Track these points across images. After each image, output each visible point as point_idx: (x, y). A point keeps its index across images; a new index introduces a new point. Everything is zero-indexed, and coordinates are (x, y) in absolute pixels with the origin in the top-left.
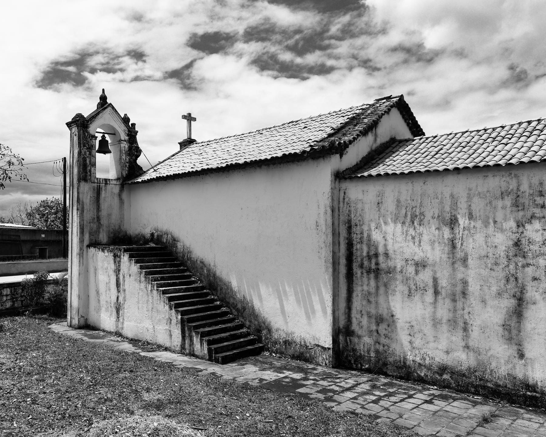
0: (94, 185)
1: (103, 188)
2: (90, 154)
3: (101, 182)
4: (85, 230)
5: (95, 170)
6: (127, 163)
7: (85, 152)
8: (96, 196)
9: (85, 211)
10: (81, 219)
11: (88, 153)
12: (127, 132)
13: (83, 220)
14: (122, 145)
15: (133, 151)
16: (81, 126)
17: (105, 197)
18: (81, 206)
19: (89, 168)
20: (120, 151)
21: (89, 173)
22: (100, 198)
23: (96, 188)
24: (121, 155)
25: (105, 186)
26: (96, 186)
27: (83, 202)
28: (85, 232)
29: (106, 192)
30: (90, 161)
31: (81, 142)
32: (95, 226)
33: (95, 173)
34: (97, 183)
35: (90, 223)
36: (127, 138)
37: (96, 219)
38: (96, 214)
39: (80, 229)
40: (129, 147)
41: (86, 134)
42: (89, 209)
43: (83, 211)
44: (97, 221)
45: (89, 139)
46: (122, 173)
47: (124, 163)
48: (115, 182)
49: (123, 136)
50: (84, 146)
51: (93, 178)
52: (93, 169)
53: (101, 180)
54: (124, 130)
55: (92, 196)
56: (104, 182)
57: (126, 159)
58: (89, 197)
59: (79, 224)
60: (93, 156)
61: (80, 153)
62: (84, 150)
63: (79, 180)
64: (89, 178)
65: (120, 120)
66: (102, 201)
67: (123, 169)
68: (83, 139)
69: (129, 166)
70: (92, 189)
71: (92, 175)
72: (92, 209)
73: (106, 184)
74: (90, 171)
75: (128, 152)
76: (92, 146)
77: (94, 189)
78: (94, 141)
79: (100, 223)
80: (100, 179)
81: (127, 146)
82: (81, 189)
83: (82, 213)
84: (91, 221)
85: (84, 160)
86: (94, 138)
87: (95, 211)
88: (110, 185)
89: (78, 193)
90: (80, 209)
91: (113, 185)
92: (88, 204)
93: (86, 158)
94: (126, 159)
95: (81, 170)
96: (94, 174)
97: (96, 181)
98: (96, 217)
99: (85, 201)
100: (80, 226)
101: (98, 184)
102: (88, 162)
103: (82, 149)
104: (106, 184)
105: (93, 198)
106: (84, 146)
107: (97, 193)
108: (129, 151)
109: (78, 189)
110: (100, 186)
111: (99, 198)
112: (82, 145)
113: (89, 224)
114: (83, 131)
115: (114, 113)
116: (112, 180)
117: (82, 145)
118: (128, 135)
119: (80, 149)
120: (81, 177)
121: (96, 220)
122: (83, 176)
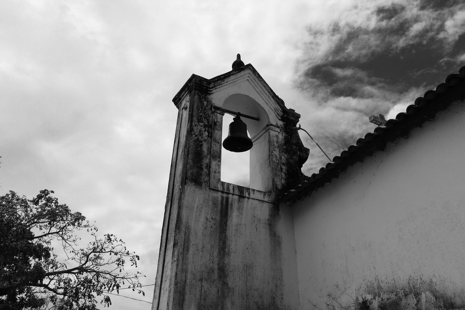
0: (215, 194)
1: (236, 205)
2: (210, 136)
3: (231, 191)
4: (187, 297)
5: (219, 166)
6: (283, 164)
7: (200, 131)
8: (218, 218)
9: (191, 252)
10: (180, 267)
11: (207, 133)
12: (281, 114)
13: (185, 271)
14: (272, 133)
15: (294, 147)
16: (196, 89)
17: (238, 225)
18: (182, 235)
19: (206, 161)
20: (269, 142)
21: (205, 170)
22: (229, 223)
23: (219, 202)
24: (272, 149)
25: (239, 201)
26: (220, 199)
27: (188, 228)
28: (186, 302)
29: (241, 214)
30: (209, 149)
31: (195, 113)
32: (214, 291)
33: (219, 172)
34: (223, 192)
35: (201, 280)
36: (280, 123)
37: (216, 272)
38: (216, 260)
39: (175, 292)
40: (285, 138)
41: (205, 103)
42: (200, 247)
43: (186, 248)
44: (220, 277)
45: (210, 112)
46: (273, 181)
47: (278, 164)
48: (260, 197)
49: (274, 119)
50: (199, 121)
51: (213, 182)
52: (214, 163)
53: (231, 188)
54: (276, 110)
55: (209, 217)
56: (237, 192)
57: (281, 158)
58: (202, 219)
59: (173, 279)
60: (215, 141)
61: (190, 131)
62: (199, 127)
63: (184, 183)
64: (206, 179)
65: (266, 92)
66: (231, 231)
67: (275, 175)
68: (198, 109)
69: (287, 170)
70: (211, 203)
71: (212, 174)
72: (209, 246)
73: (241, 196)
74: (209, 166)
75: (285, 147)
76: (215, 124)
77: (215, 204)
78: (218, 115)
79: (225, 284)
80: (229, 184)
81: (281, 137)
82: (187, 199)
83: (183, 253)
84: (205, 276)
85: (199, 144)
86: (218, 111)
87: (216, 254)
88: (250, 200)
89: (180, 208)
90: (180, 242)
91: (257, 202)
92: (200, 234)
93: (201, 142)
94: (281, 158)
95: (190, 161)
96: (217, 174)
97: (220, 188)
98: (216, 267)
99: (192, 224)
100: (176, 284)
101: (225, 195)
102: (205, 148)
103: (196, 125)
104: (241, 196)
105: (213, 222)
106: (199, 121)
107: (221, 212)
108: (285, 144)
109: (180, 199)
110: (227, 198)
111: (226, 223)
112: (195, 119)
113: (199, 284)
114: (200, 98)
115: (257, 80)
116: (254, 190)
117: (195, 119)
118: (282, 119)
119: (191, 126)
120: (189, 174)
121: (216, 276)
122: (192, 174)
